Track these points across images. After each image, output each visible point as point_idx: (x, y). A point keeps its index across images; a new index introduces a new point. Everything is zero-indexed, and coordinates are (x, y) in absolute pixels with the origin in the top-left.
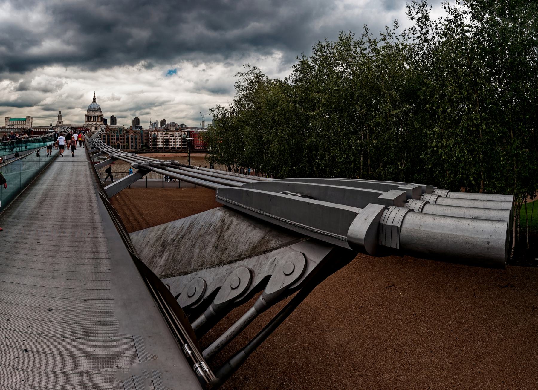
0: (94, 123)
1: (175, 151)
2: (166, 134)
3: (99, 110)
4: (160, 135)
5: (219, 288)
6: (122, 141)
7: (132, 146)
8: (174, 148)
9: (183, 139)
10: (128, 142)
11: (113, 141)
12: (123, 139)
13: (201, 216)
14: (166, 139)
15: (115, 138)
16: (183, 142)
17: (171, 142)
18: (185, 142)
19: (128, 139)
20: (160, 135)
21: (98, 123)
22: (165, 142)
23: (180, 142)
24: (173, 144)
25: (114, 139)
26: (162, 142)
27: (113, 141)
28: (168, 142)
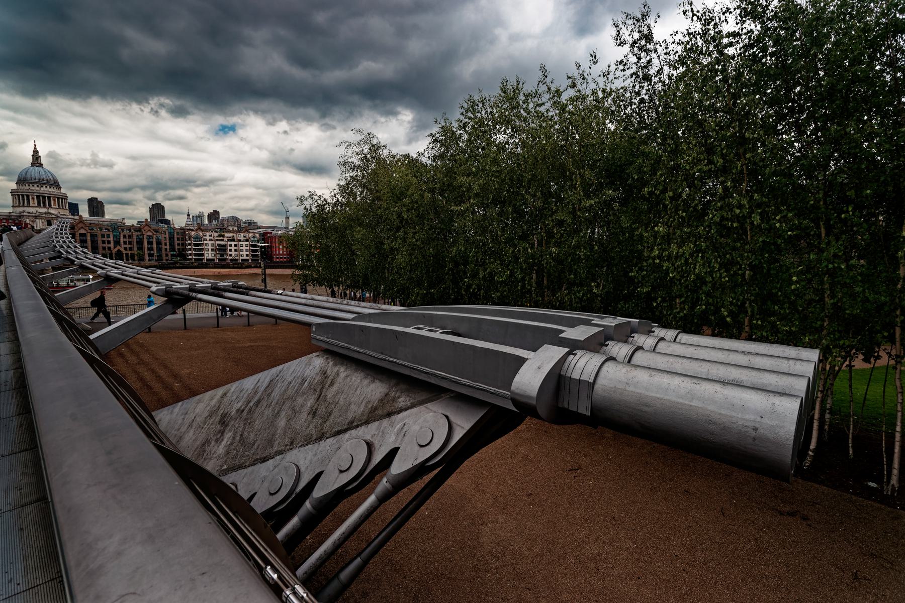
0: (43, 210)
1: (236, 264)
2: (219, 236)
3: (55, 184)
4: (208, 238)
5: (319, 475)
6: (128, 246)
7: (150, 255)
8: (236, 260)
9: (252, 246)
10: (141, 248)
11: (106, 245)
12: (130, 243)
13: (288, 368)
14: (219, 245)
15: (111, 239)
16: (252, 251)
17: (231, 250)
18: (257, 251)
19: (140, 242)
20: (208, 238)
21: (51, 211)
22: (219, 250)
23: (247, 250)
24: (233, 253)
25: (109, 242)
26: (213, 250)
27: (106, 245)
28: (225, 250)
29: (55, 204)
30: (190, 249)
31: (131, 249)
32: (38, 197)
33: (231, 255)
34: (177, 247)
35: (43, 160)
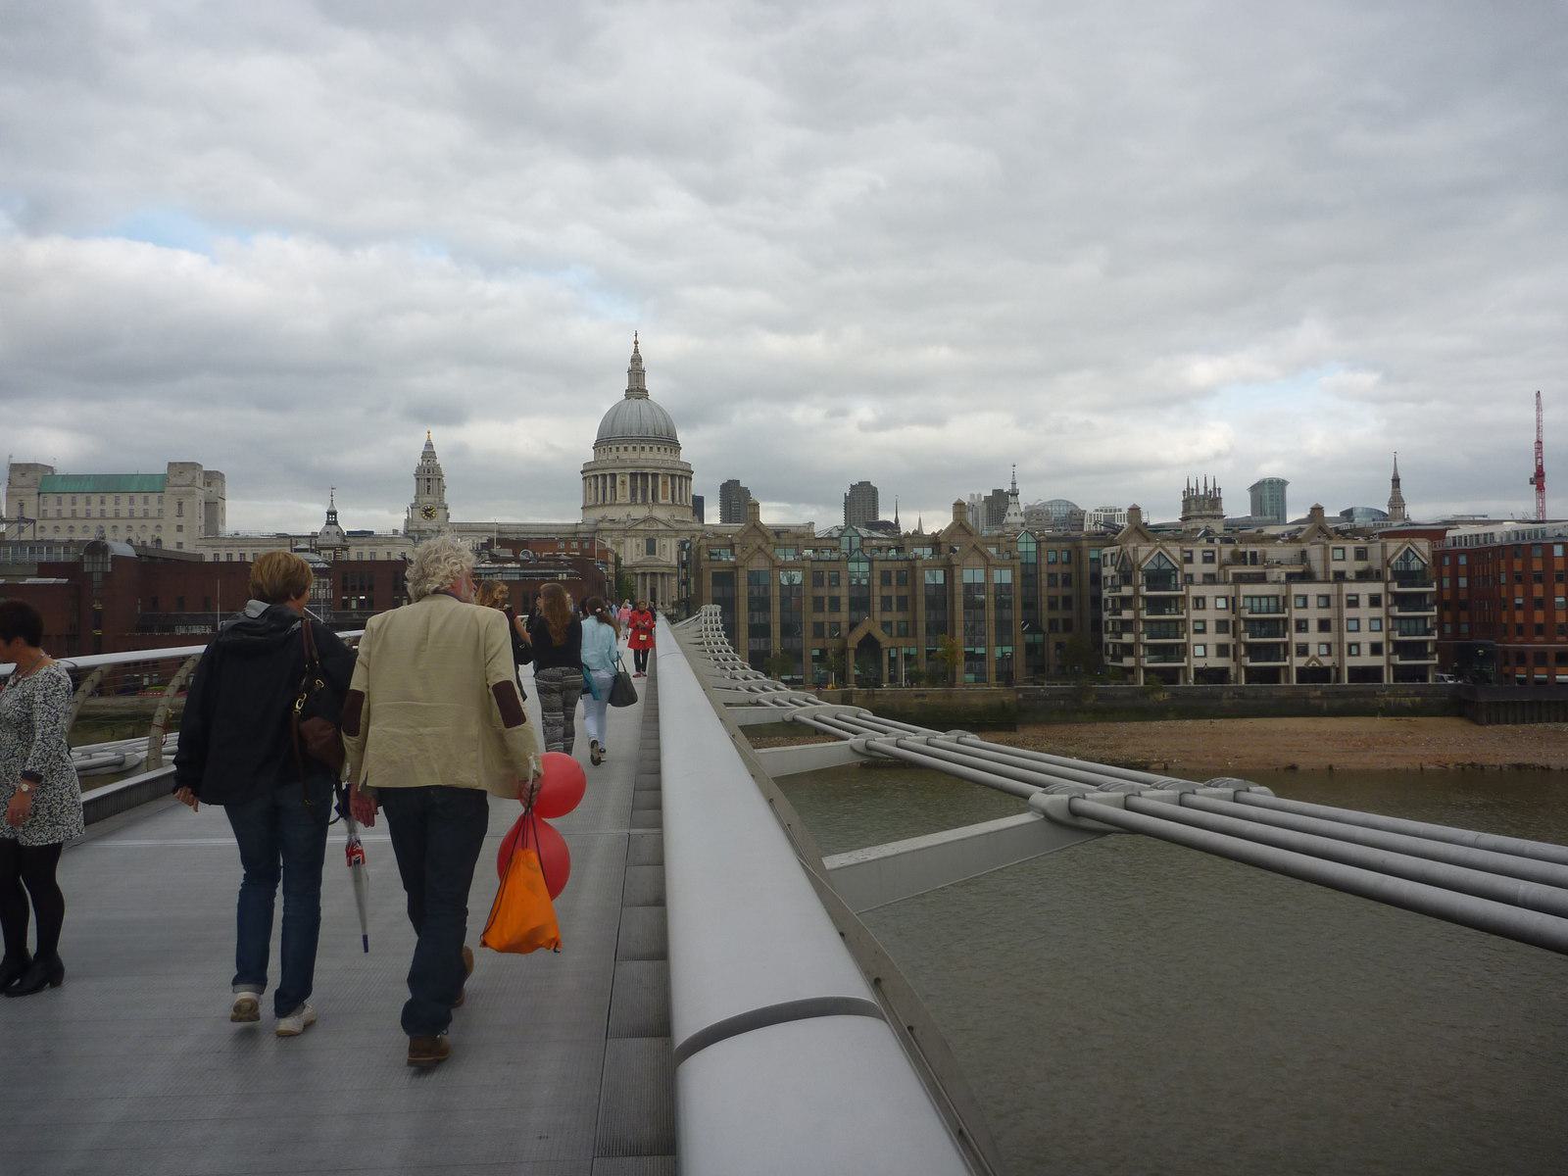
0: (639, 512)
6: (894, 616)
9: (1401, 600)
12: (903, 604)
15: (843, 593)
17: (1302, 626)
20: (1198, 568)
21: (660, 513)
24: (1313, 638)
25: (835, 603)
26: (1222, 626)
28: (1277, 627)
30: (1127, 626)
31: (907, 631)
33: (1303, 650)
34: (1046, 615)
35: (650, 384)
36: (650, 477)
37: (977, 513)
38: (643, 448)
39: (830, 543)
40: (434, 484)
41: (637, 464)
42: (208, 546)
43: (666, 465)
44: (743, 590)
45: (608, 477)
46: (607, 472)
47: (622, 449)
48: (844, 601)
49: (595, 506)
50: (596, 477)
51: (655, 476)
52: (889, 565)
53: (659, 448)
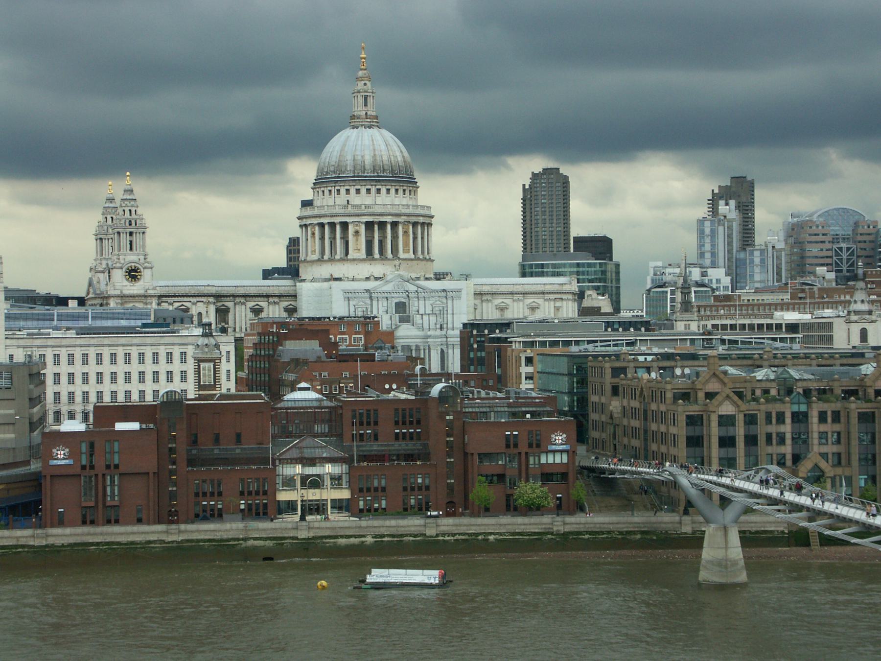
15: (787, 428)
25: (782, 440)
29: (406, 251)
32: (369, 225)
36: (389, 227)
37: (730, 228)
38: (379, 191)
39: (768, 385)
40: (136, 239)
41: (371, 210)
42: (19, 347)
43: (407, 211)
44: (715, 431)
45: (338, 228)
46: (337, 220)
47: (353, 191)
48: (788, 436)
49: (321, 260)
50: (322, 225)
51: (395, 225)
52: (824, 406)
53: (397, 190)
